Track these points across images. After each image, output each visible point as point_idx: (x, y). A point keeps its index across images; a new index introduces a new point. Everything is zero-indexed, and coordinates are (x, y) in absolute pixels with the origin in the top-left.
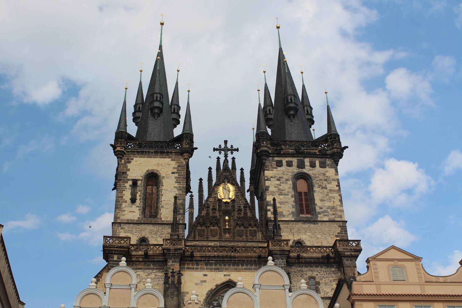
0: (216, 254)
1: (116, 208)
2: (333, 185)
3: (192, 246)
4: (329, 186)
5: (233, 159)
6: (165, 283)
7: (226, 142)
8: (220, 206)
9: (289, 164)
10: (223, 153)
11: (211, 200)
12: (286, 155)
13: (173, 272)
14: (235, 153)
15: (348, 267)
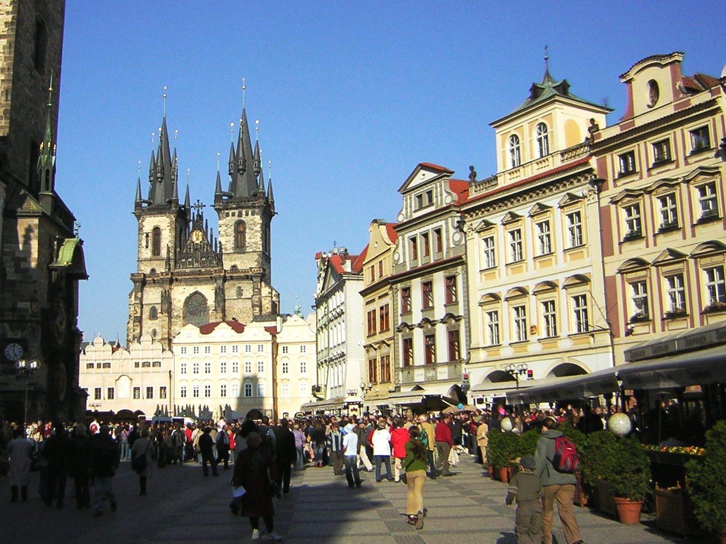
0: (189, 277)
1: (139, 251)
2: (258, 228)
3: (177, 272)
4: (255, 228)
5: (202, 212)
6: (162, 297)
7: (198, 201)
8: (193, 246)
9: (233, 215)
10: (196, 209)
11: (189, 242)
12: (232, 209)
13: (165, 291)
14: (203, 208)
15: (255, 282)
